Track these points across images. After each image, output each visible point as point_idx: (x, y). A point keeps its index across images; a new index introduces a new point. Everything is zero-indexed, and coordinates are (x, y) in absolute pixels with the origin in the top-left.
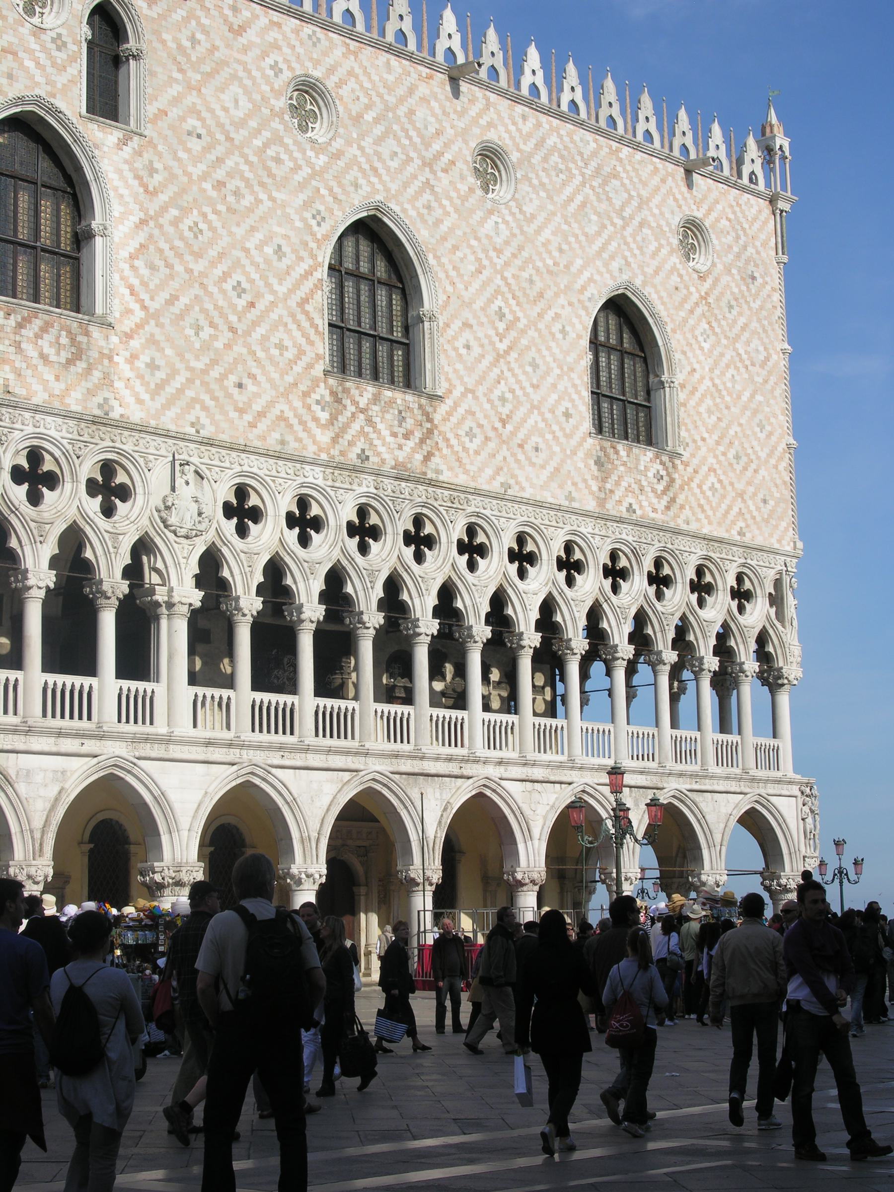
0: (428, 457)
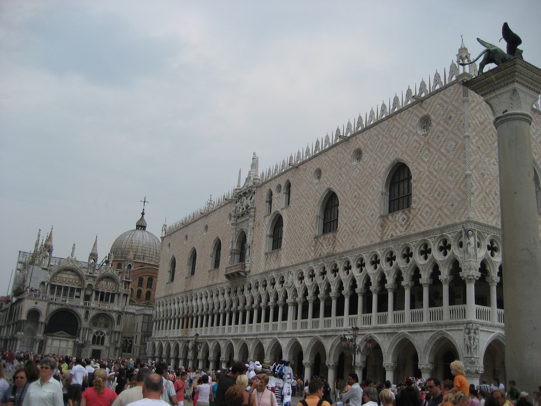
0: (334, 249)
